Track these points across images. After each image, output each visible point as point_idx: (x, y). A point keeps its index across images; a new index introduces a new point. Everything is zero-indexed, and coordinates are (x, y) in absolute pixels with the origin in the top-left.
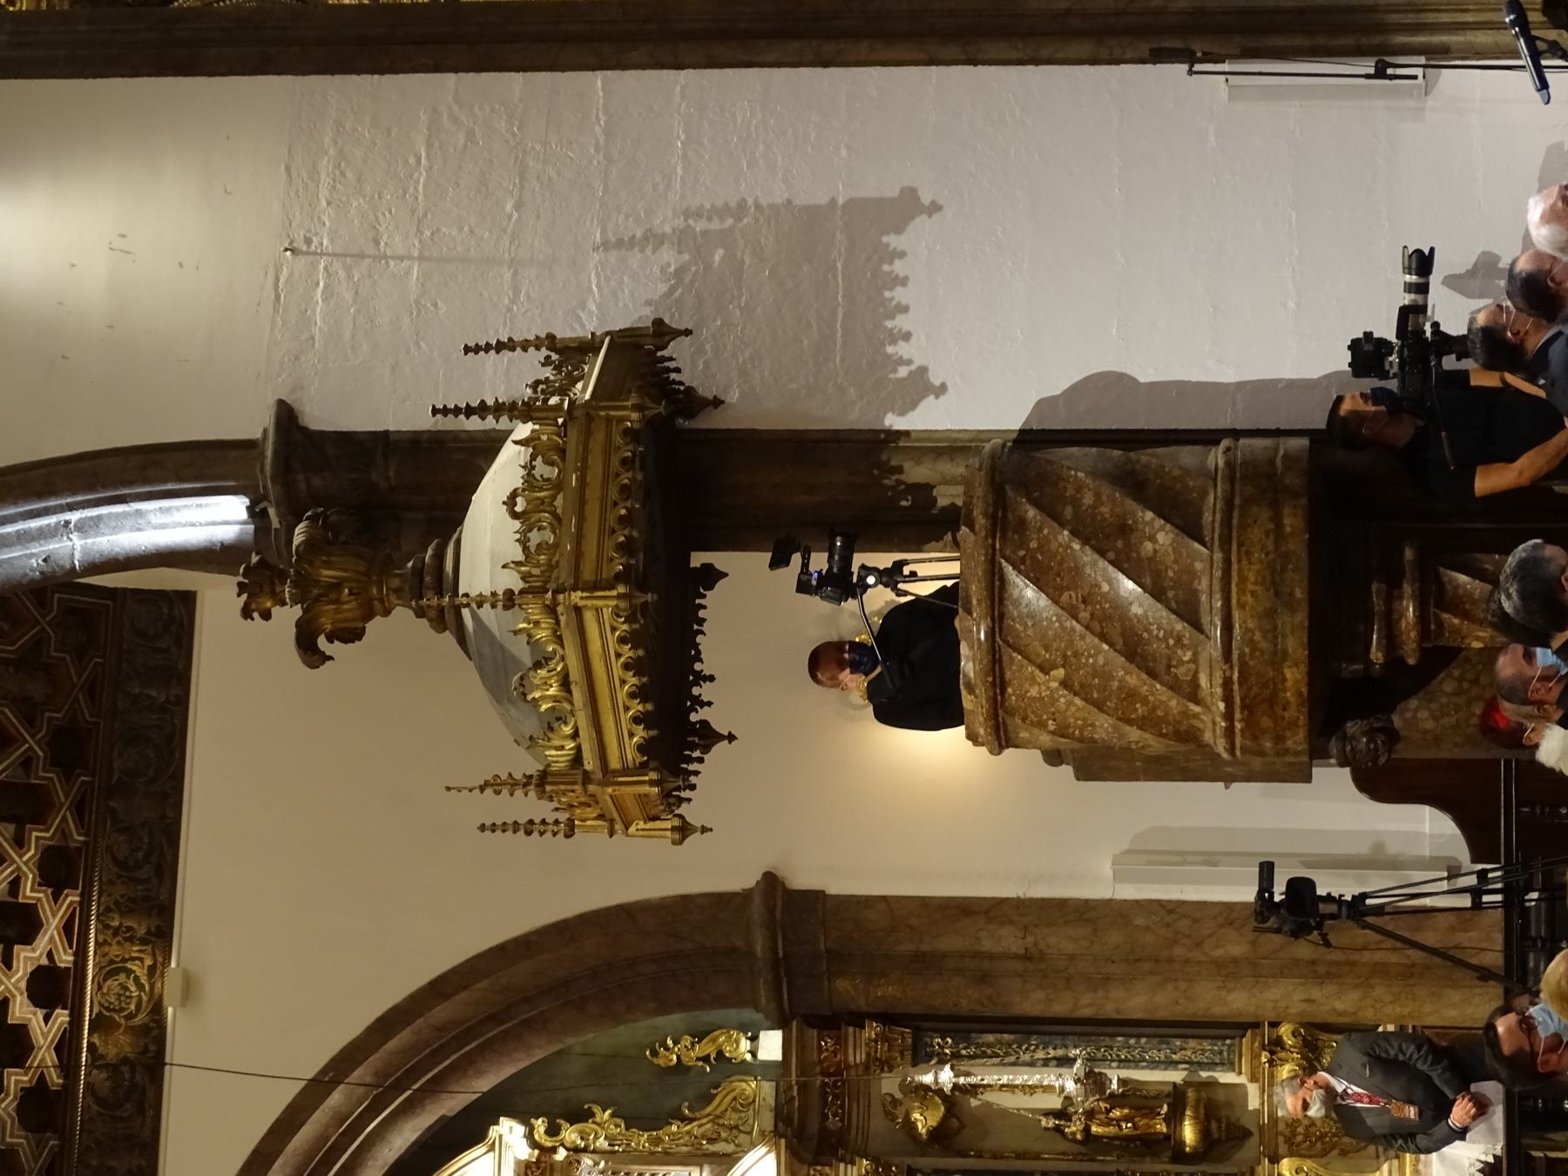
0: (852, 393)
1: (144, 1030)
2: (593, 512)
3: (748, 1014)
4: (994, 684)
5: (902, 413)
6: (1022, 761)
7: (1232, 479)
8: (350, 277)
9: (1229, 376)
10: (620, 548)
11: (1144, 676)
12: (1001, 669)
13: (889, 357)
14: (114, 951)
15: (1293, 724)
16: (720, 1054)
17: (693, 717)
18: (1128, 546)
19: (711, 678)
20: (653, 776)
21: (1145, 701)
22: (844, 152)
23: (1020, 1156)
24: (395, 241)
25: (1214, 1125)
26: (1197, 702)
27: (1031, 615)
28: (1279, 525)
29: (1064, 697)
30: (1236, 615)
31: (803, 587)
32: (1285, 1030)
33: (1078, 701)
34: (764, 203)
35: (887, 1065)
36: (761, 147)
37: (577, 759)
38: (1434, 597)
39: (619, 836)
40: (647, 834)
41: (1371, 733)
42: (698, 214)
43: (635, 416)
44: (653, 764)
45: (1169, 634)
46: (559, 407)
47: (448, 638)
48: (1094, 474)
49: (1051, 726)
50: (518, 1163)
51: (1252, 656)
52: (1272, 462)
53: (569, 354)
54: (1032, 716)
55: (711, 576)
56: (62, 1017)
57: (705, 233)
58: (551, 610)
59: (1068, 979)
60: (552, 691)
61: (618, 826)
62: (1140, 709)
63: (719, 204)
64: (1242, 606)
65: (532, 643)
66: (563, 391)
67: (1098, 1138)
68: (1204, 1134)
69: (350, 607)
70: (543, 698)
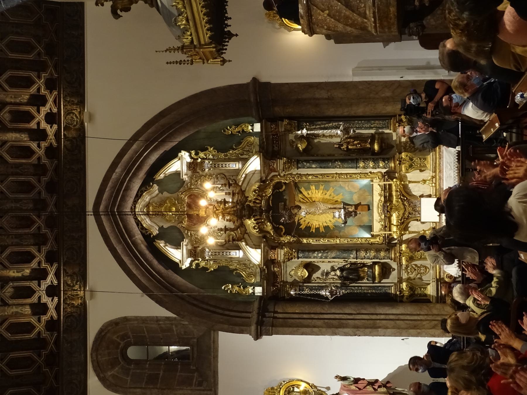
1: (79, 130)
3: (251, 119)
4: (308, 16)
6: (318, 39)
11: (351, 12)
12: (311, 11)
14: (69, 107)
16: (243, 130)
17: (226, 30)
19: (230, 18)
21: (351, 19)
23: (328, 155)
25: (383, 144)
26: (366, 19)
33: (332, 20)
35: (290, 131)
39: (206, 64)
40: (214, 63)
44: (213, 42)
47: (154, 9)
49: (325, 27)
50: (187, 163)
54: (320, 25)
56: (55, 127)
60: (184, 22)
61: (205, 61)
62: (350, 21)
65: (178, 9)
67: (351, 149)
68: (380, 147)
70: (182, 24)
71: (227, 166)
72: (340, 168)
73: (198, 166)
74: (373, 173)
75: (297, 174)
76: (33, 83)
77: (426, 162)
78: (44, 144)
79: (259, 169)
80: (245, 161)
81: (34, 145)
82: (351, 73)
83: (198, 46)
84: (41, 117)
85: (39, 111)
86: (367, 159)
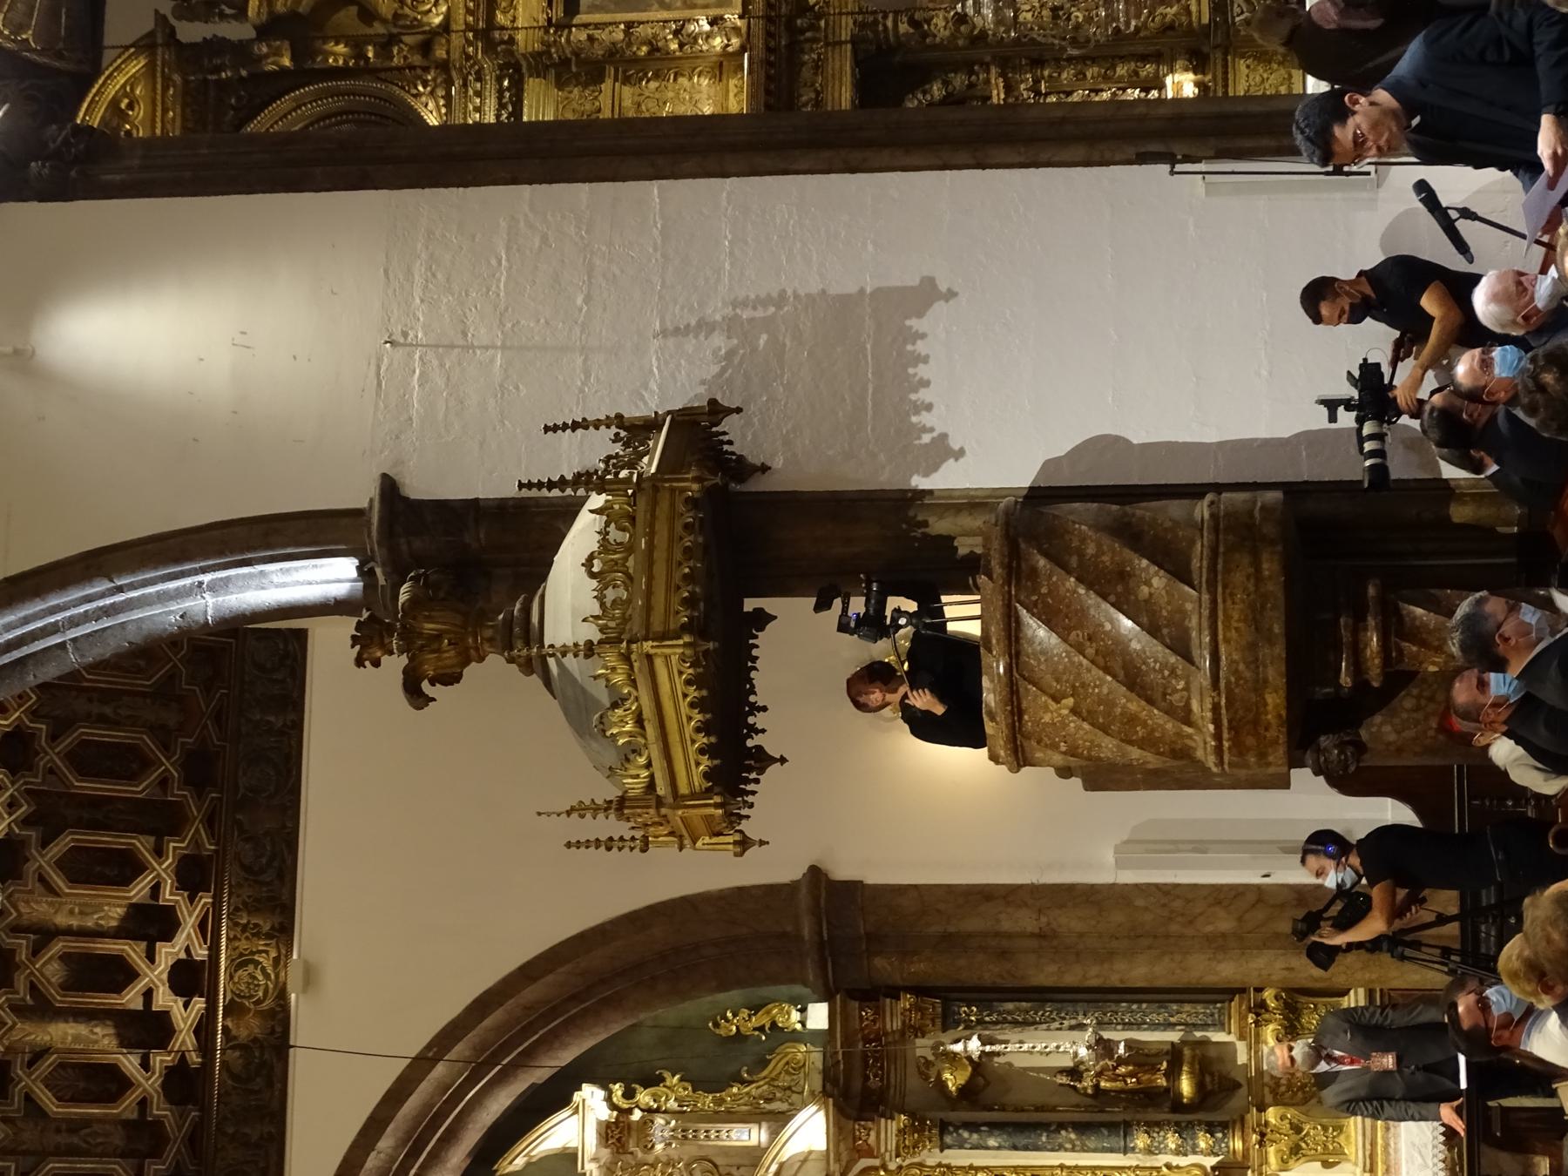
0: (882, 457)
1: (271, 1014)
2: (660, 569)
3: (798, 989)
4: (1012, 712)
5: (926, 475)
7: (1215, 529)
8: (442, 365)
9: (1211, 436)
10: (685, 602)
12: (1019, 699)
13: (913, 425)
14: (243, 945)
15: (1275, 742)
16: (774, 1024)
17: (750, 743)
18: (1128, 591)
19: (764, 709)
20: (718, 799)
21: (1145, 725)
22: (870, 247)
23: (1039, 1109)
24: (481, 333)
25: (1208, 1079)
26: (1189, 723)
27: (1043, 652)
28: (1258, 570)
29: (1073, 723)
30: (1222, 649)
31: (843, 627)
32: (1268, 995)
33: (1086, 726)
34: (802, 293)
35: (920, 1031)
36: (799, 245)
37: (651, 786)
38: (1395, 627)
41: (1341, 746)
42: (744, 304)
43: (695, 486)
44: (717, 789)
45: (1164, 665)
46: (628, 480)
47: (535, 680)
48: (1096, 527)
50: (599, 1123)
51: (1237, 685)
52: (1250, 513)
53: (636, 431)
55: (762, 619)
56: (199, 1004)
57: (751, 320)
58: (626, 658)
59: (1077, 954)
60: (628, 728)
61: (687, 842)
62: (1141, 732)
63: (763, 295)
64: (1227, 641)
65: (610, 687)
66: (631, 465)
67: (1106, 1092)
68: (1199, 1086)
69: (450, 655)
70: (620, 734)
71: (724, 1135)
72: (1073, 1150)
73: (634, 1134)
74: (1178, 1167)
75: (940, 1165)
76: (139, 868)
77: (1342, 1139)
78: (160, 1060)
79: (823, 1147)
80: (778, 1120)
81: (130, 1063)
82: (1110, 857)
83: (670, 800)
84: (156, 975)
85: (151, 957)
86: (1159, 1125)
